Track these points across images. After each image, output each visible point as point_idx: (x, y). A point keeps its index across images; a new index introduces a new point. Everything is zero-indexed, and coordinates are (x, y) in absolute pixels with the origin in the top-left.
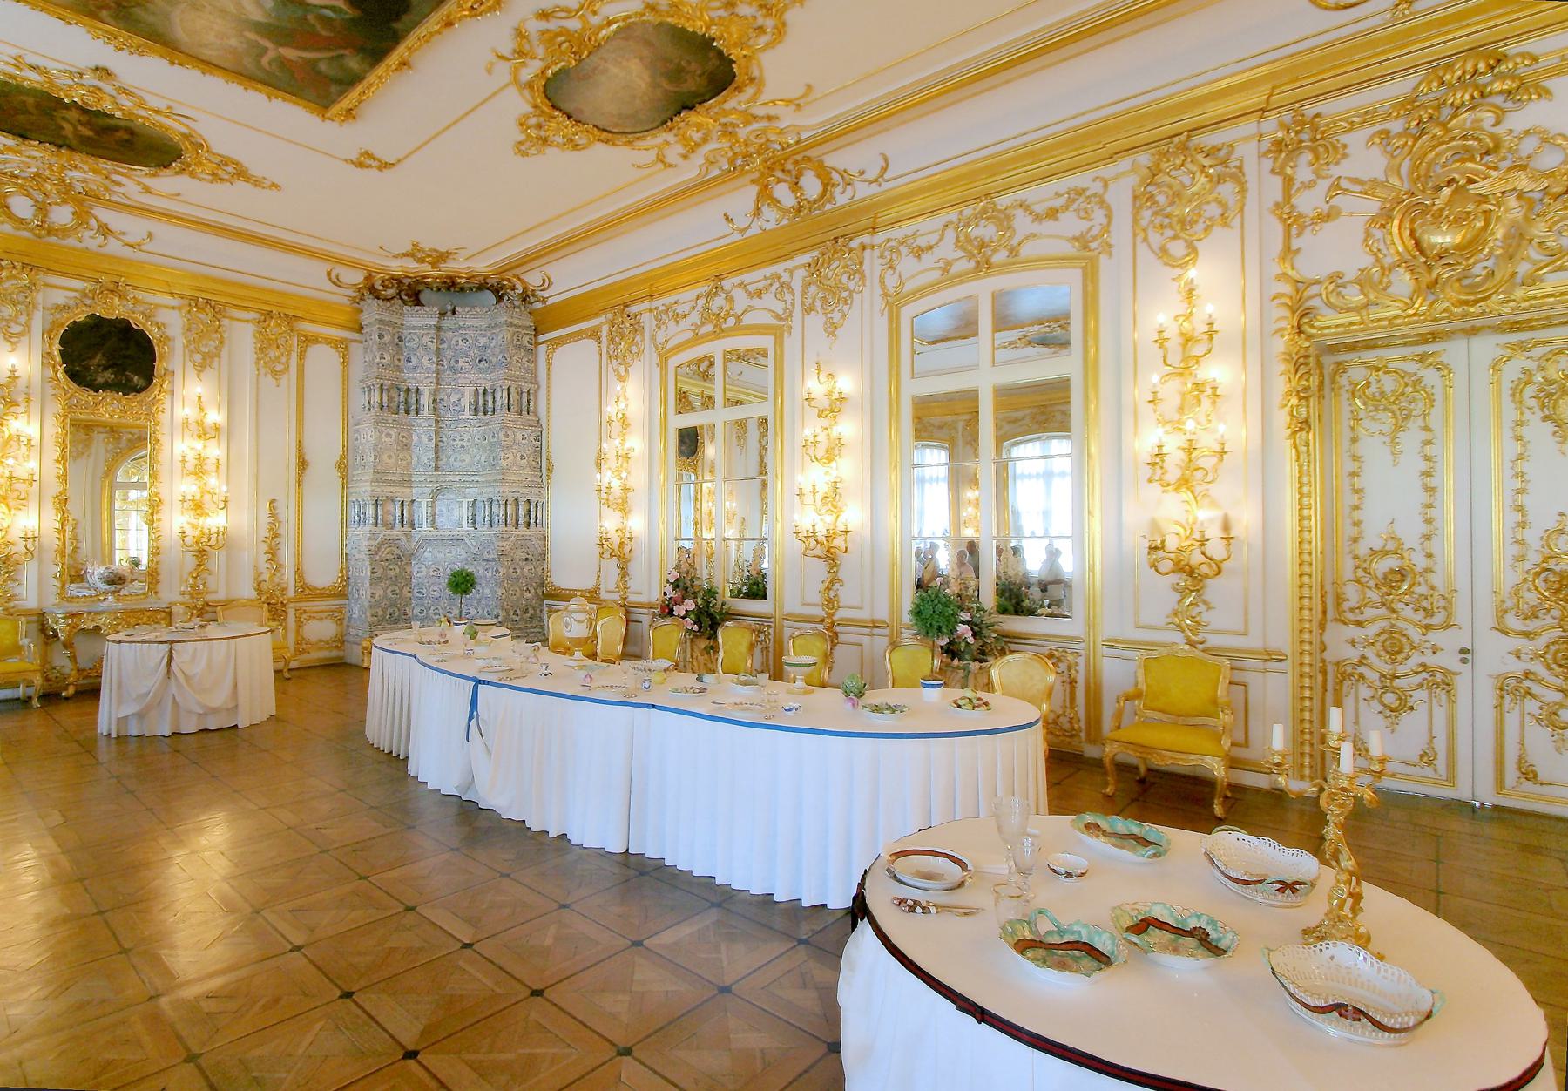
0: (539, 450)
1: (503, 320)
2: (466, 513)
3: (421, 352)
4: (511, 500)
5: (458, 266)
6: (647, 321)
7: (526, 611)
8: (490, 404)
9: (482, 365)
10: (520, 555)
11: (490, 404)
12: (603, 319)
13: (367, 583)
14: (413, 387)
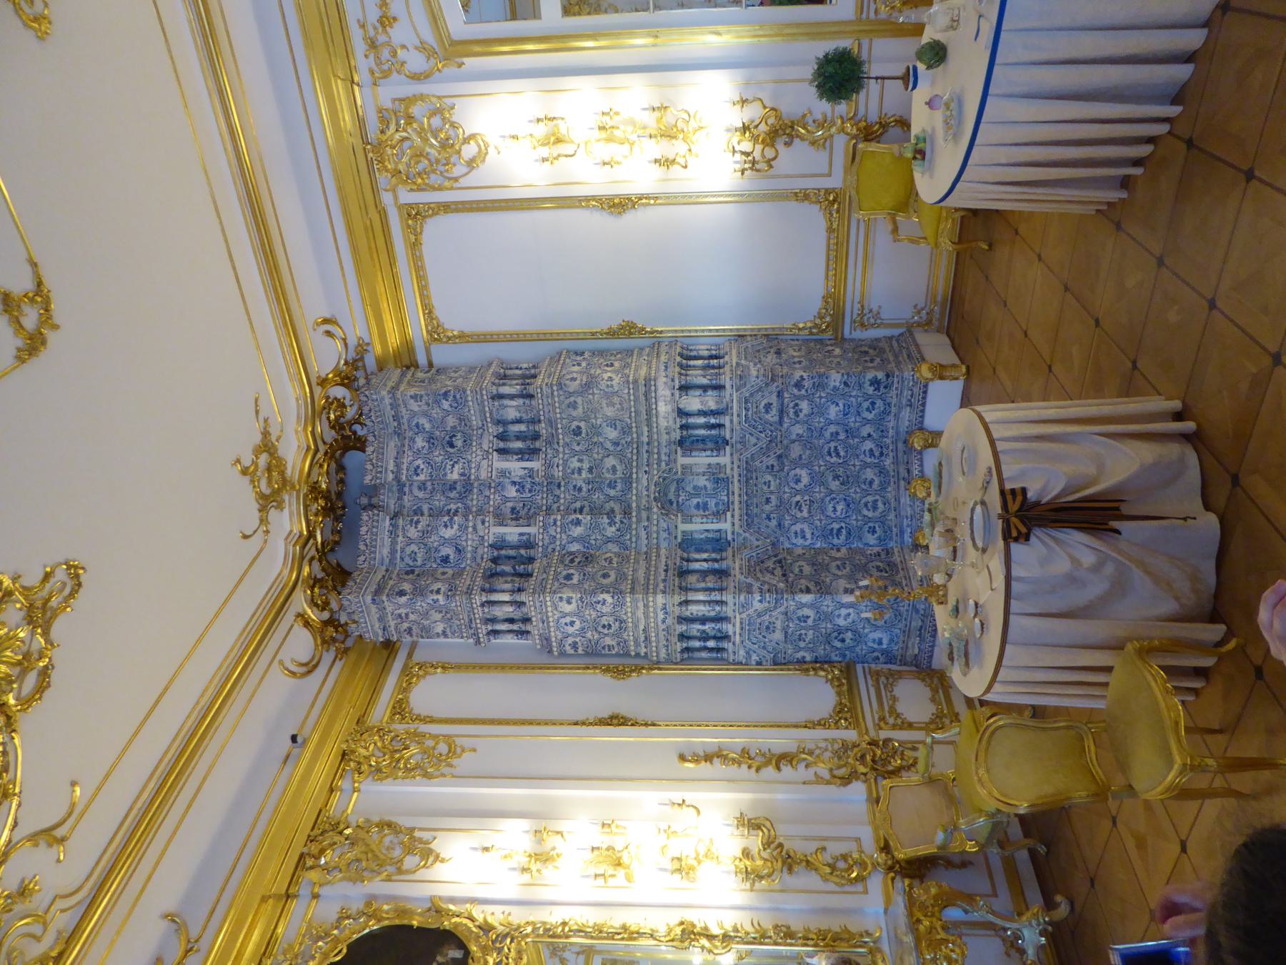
0: (601, 353)
1: (387, 401)
2: (701, 460)
3: (433, 540)
4: (677, 369)
5: (295, 452)
6: (389, 92)
7: (866, 353)
8: (523, 427)
9: (459, 443)
10: (771, 359)
11: (523, 427)
12: (387, 198)
13: (827, 603)
14: (486, 553)
